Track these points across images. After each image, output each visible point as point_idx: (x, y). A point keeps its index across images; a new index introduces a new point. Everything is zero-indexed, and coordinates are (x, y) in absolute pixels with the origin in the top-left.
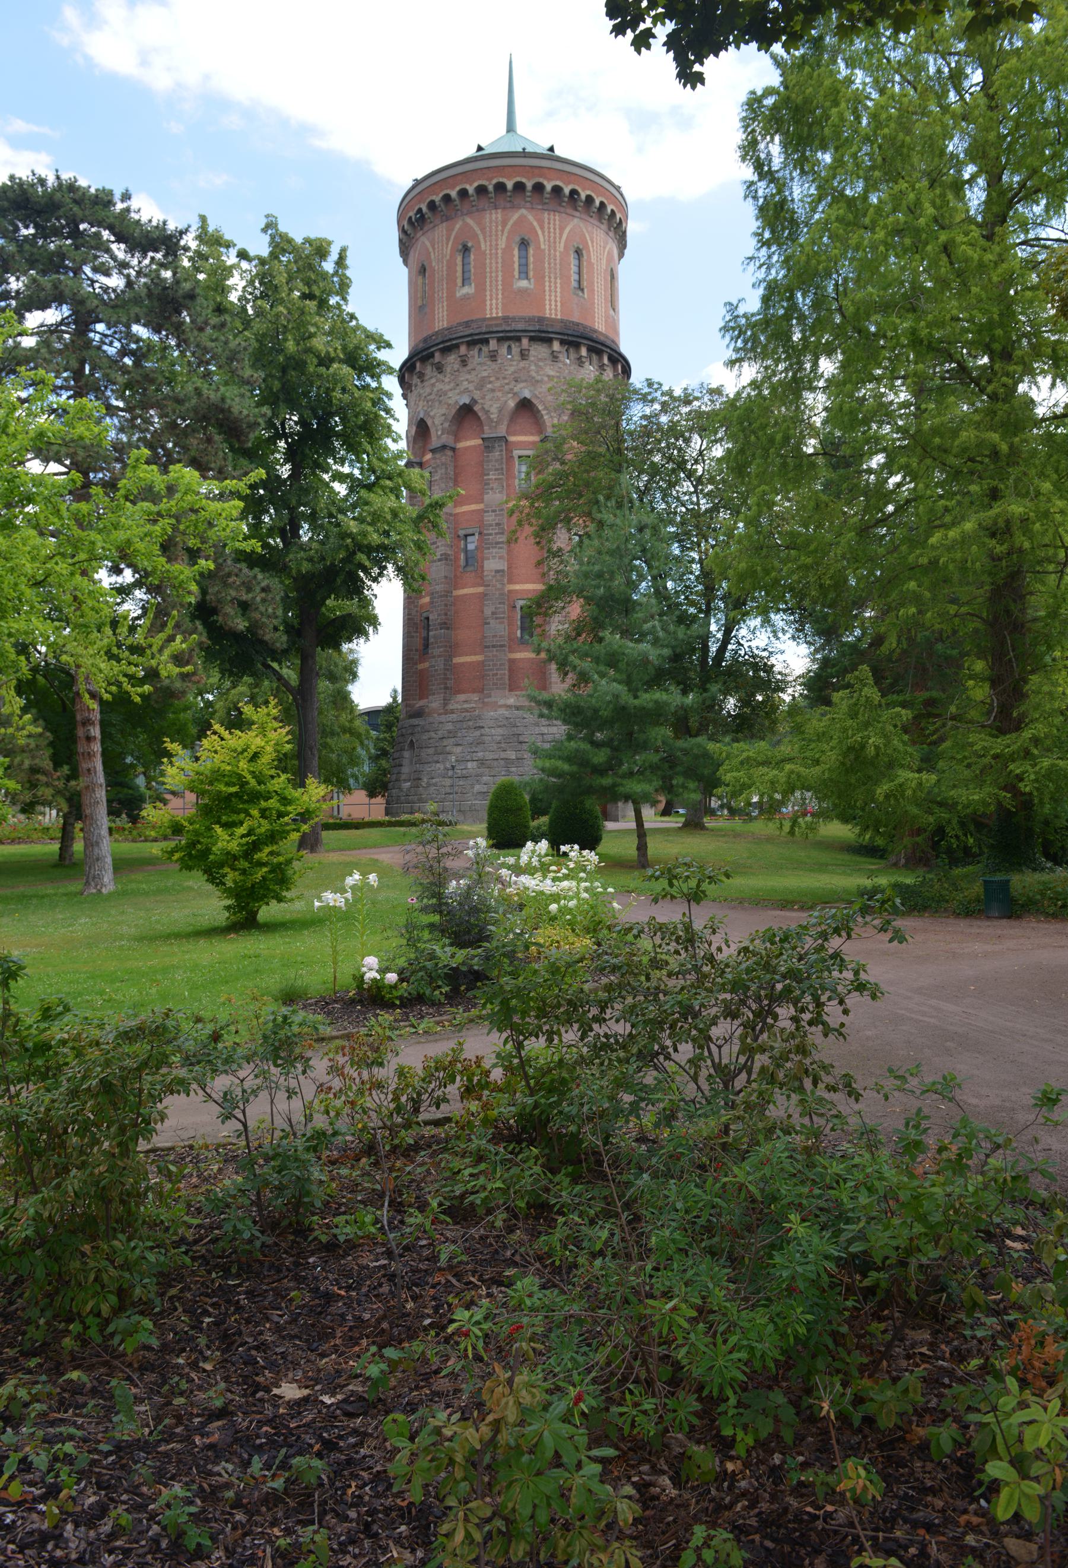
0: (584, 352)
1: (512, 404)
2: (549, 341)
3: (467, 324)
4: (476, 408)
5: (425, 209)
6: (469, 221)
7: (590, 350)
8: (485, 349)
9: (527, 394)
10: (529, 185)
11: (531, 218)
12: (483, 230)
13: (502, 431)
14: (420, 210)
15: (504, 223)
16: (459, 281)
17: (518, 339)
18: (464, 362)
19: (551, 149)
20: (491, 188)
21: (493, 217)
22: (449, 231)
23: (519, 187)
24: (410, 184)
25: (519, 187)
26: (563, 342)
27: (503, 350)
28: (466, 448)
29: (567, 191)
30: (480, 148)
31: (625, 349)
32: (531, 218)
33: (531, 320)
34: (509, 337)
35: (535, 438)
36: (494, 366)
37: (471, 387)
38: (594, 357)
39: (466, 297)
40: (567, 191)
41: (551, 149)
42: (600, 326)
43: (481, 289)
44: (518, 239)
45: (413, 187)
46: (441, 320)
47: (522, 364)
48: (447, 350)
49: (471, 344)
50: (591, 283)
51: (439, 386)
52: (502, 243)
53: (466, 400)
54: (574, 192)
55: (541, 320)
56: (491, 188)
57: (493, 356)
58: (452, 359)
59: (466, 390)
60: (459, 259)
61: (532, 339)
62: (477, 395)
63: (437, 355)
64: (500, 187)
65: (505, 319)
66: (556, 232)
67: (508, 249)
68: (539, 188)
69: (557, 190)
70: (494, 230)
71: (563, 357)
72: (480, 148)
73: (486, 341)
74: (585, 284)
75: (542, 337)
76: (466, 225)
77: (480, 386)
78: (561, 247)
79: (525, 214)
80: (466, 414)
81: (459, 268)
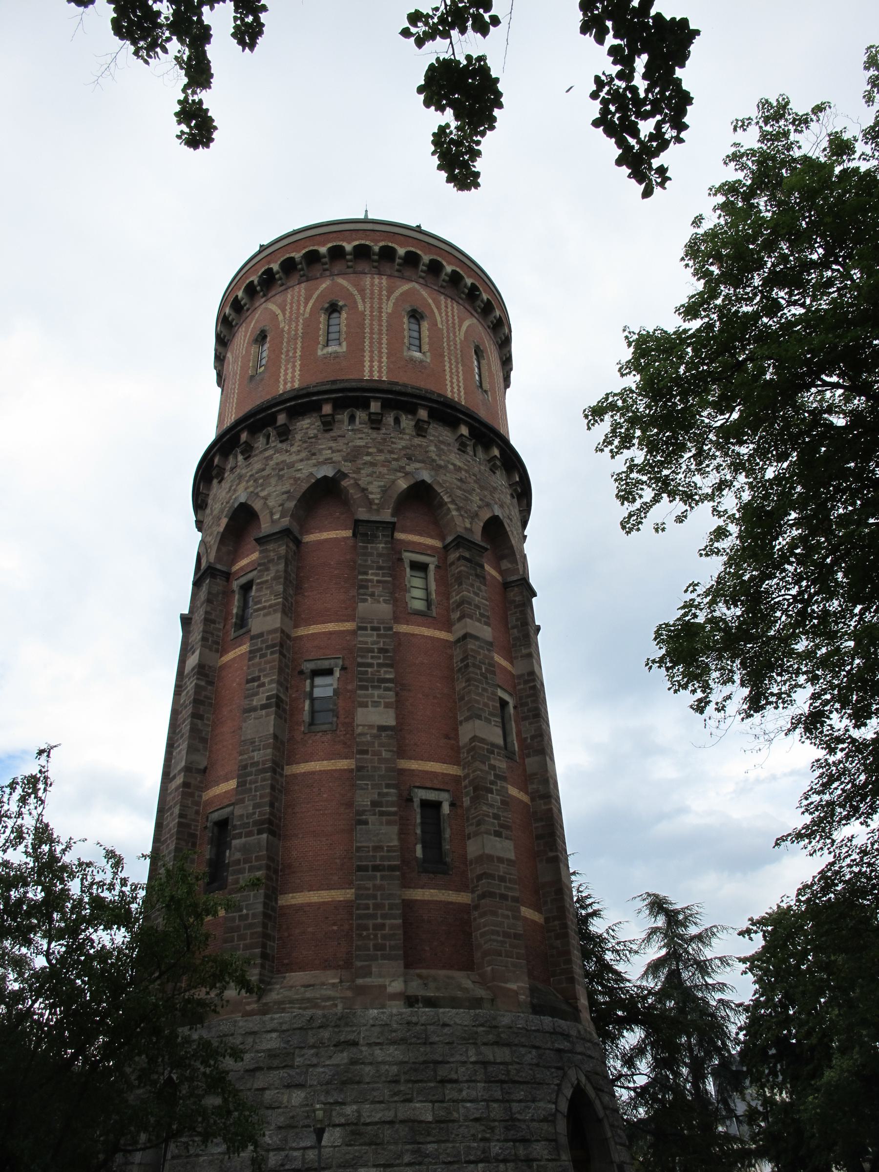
1: (403, 484)
4: (345, 483)
6: (341, 281)
9: (426, 476)
12: (362, 291)
15: (390, 292)
23: (412, 259)
24: (258, 249)
35: (437, 544)
36: (374, 434)
37: (337, 457)
45: (260, 252)
47: (417, 441)
49: (340, 405)
51: (278, 458)
53: (328, 471)
57: (375, 423)
58: (307, 425)
59: (328, 461)
62: (347, 467)
71: (470, 450)
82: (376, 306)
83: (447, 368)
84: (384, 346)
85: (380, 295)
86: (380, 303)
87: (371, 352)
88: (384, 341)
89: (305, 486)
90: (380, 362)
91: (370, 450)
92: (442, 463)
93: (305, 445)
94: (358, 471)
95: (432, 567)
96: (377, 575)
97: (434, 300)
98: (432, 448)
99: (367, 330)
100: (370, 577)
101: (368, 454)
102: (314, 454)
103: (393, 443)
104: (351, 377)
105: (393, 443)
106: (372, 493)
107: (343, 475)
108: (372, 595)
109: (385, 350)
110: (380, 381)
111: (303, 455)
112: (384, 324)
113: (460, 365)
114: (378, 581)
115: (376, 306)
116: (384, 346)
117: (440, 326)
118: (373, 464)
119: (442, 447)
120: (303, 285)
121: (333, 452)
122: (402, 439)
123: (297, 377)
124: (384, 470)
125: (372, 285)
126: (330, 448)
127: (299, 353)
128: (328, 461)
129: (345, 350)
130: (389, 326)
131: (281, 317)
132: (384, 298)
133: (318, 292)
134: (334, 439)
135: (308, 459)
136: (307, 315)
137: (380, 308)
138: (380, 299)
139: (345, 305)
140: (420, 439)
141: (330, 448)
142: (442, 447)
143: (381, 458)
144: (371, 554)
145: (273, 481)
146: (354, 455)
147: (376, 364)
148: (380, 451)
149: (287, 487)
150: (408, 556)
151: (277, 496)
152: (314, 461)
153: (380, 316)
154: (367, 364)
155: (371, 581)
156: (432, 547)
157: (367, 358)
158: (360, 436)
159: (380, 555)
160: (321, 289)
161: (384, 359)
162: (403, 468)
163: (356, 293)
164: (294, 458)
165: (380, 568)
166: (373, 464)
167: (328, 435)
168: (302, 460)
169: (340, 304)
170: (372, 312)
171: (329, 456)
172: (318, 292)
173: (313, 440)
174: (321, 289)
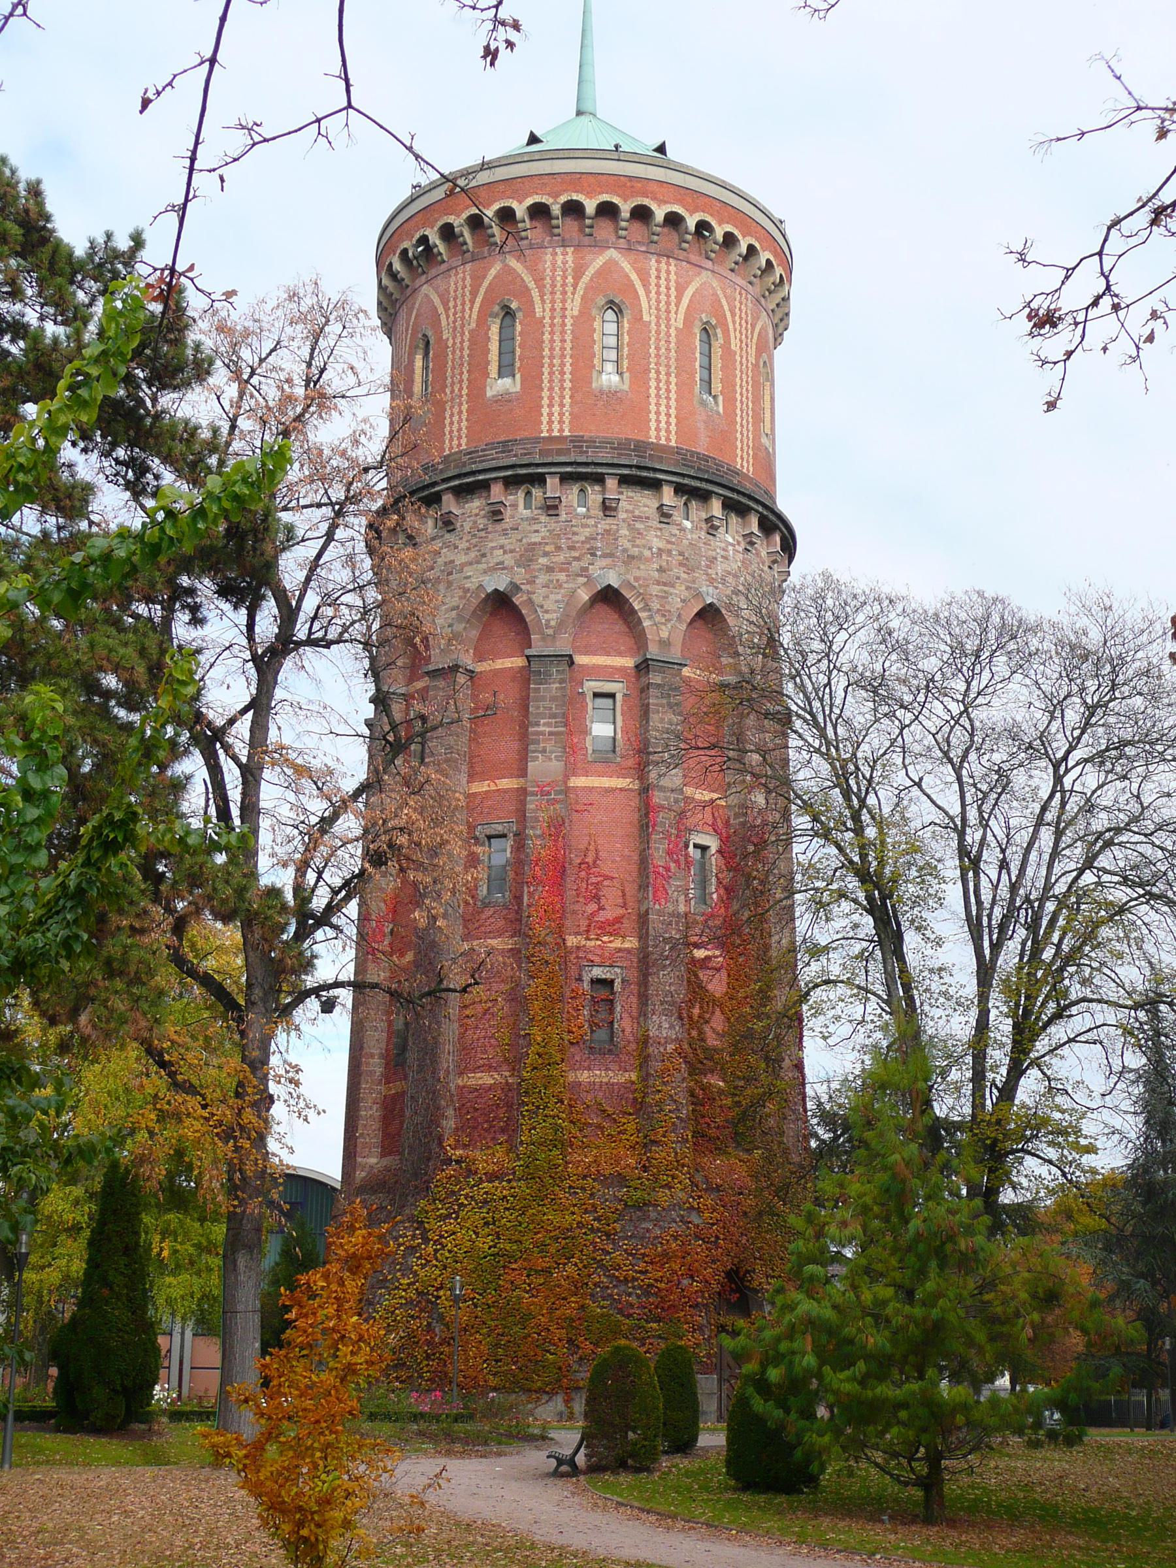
0: (716, 507)
1: (584, 596)
2: (655, 485)
3: (506, 446)
4: (517, 600)
5: (434, 238)
7: (728, 505)
8: (537, 492)
10: (625, 209)
11: (626, 266)
12: (539, 281)
13: (562, 645)
14: (424, 240)
15: (578, 274)
16: (493, 369)
17: (599, 479)
18: (496, 515)
19: (661, 149)
20: (556, 210)
21: (558, 260)
22: (477, 280)
23: (607, 210)
24: (407, 193)
25: (607, 210)
26: (679, 490)
27: (571, 495)
28: (497, 673)
29: (691, 223)
30: (533, 139)
31: (785, 504)
32: (626, 266)
33: (621, 446)
34: (584, 475)
36: (552, 523)
37: (509, 560)
38: (734, 519)
39: (504, 399)
40: (691, 223)
41: (661, 149)
42: (744, 463)
43: (532, 383)
44: (601, 301)
45: (412, 200)
46: (457, 436)
47: (605, 524)
48: (464, 492)
49: (511, 483)
50: (729, 386)
52: (574, 307)
53: (498, 582)
54: (702, 226)
55: (641, 447)
56: (556, 210)
57: (551, 508)
59: (500, 566)
60: (494, 330)
61: (624, 481)
63: (448, 499)
64: (573, 209)
65: (577, 442)
66: (669, 290)
67: (584, 319)
68: (642, 214)
69: (673, 220)
70: (559, 279)
71: (677, 516)
72: (533, 139)
73: (540, 480)
74: (717, 387)
75: (642, 480)
76: (508, 270)
77: (527, 556)
78: (678, 321)
79: (611, 257)
80: (501, 606)
81: (494, 346)
82: (558, 306)
83: (653, 391)
84: (568, 376)
85: (564, 285)
86: (564, 301)
87: (551, 389)
88: (568, 369)
89: (475, 602)
90: (562, 405)
91: (547, 548)
92: (635, 551)
93: (474, 541)
94: (531, 582)
95: (619, 697)
96: (548, 725)
97: (639, 272)
98: (624, 532)
99: (546, 352)
100: (541, 729)
101: (546, 554)
102: (484, 555)
103: (575, 534)
104: (525, 434)
105: (575, 534)
106: (547, 612)
107: (516, 588)
108: (544, 751)
109: (568, 384)
110: (561, 439)
111: (473, 554)
112: (568, 337)
113: (673, 380)
114: (551, 734)
115: (558, 306)
116: (568, 376)
117: (646, 318)
118: (549, 569)
119: (638, 525)
120: (468, 266)
121: (505, 552)
122: (587, 526)
123: (464, 430)
124: (562, 577)
125: (554, 264)
126: (502, 547)
127: (465, 392)
128: (500, 566)
129: (518, 388)
130: (575, 339)
131: (443, 317)
132: (570, 289)
133: (486, 284)
134: (505, 533)
135: (478, 562)
136: (473, 325)
137: (564, 309)
138: (564, 293)
139: (519, 309)
140: (609, 520)
141: (502, 547)
142: (638, 525)
143: (561, 558)
144: (543, 699)
145: (442, 587)
146: (527, 556)
147: (556, 409)
148: (558, 548)
149: (455, 601)
150: (591, 686)
151: (447, 611)
152: (484, 566)
153: (564, 324)
154: (545, 411)
155: (543, 733)
156: (622, 670)
157: (545, 402)
158: (536, 527)
159: (553, 699)
160: (490, 277)
161: (567, 401)
162: (586, 569)
163: (532, 285)
164: (461, 559)
165: (553, 716)
166: (549, 569)
167: (499, 527)
168: (471, 564)
169: (514, 306)
170: (552, 318)
171: (500, 559)
172: (486, 284)
173: (483, 534)
174: (490, 277)
